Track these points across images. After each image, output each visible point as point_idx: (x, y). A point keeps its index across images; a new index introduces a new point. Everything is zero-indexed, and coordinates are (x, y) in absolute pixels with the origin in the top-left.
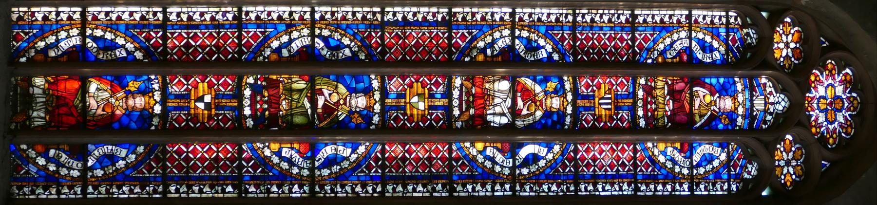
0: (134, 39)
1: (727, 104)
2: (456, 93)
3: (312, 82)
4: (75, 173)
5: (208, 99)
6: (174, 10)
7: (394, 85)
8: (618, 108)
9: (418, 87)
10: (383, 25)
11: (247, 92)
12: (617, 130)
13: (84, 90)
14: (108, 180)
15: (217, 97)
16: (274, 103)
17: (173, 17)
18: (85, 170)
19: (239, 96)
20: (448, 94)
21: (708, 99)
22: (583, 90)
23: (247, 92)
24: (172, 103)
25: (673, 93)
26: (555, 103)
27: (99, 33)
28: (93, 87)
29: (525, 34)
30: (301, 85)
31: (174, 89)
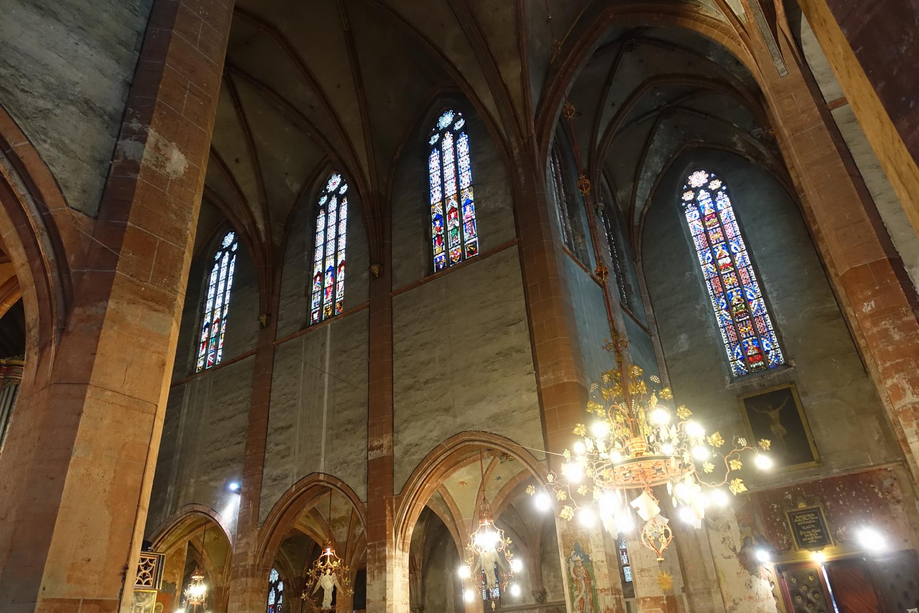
0: (734, 349)
1: (707, 206)
2: (726, 272)
3: (733, 306)
4: (773, 351)
5: (745, 328)
6: (725, 342)
7: (728, 287)
8: (717, 232)
9: (727, 282)
10: (714, 294)
11: (740, 320)
12: (722, 230)
13: (751, 356)
14: (773, 344)
15: (743, 326)
16: (741, 313)
17: (727, 342)
18: (772, 350)
19: (742, 321)
20: (726, 274)
21: (707, 210)
22: (715, 242)
23: (740, 320)
24: (748, 336)
25: (709, 220)
26: (720, 248)
27: (735, 357)
28: (749, 354)
29: (706, 261)
30: (735, 308)
31: (745, 336)
